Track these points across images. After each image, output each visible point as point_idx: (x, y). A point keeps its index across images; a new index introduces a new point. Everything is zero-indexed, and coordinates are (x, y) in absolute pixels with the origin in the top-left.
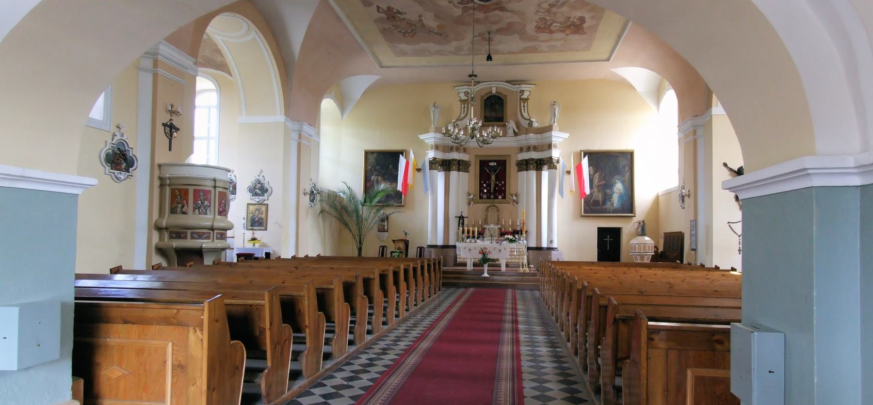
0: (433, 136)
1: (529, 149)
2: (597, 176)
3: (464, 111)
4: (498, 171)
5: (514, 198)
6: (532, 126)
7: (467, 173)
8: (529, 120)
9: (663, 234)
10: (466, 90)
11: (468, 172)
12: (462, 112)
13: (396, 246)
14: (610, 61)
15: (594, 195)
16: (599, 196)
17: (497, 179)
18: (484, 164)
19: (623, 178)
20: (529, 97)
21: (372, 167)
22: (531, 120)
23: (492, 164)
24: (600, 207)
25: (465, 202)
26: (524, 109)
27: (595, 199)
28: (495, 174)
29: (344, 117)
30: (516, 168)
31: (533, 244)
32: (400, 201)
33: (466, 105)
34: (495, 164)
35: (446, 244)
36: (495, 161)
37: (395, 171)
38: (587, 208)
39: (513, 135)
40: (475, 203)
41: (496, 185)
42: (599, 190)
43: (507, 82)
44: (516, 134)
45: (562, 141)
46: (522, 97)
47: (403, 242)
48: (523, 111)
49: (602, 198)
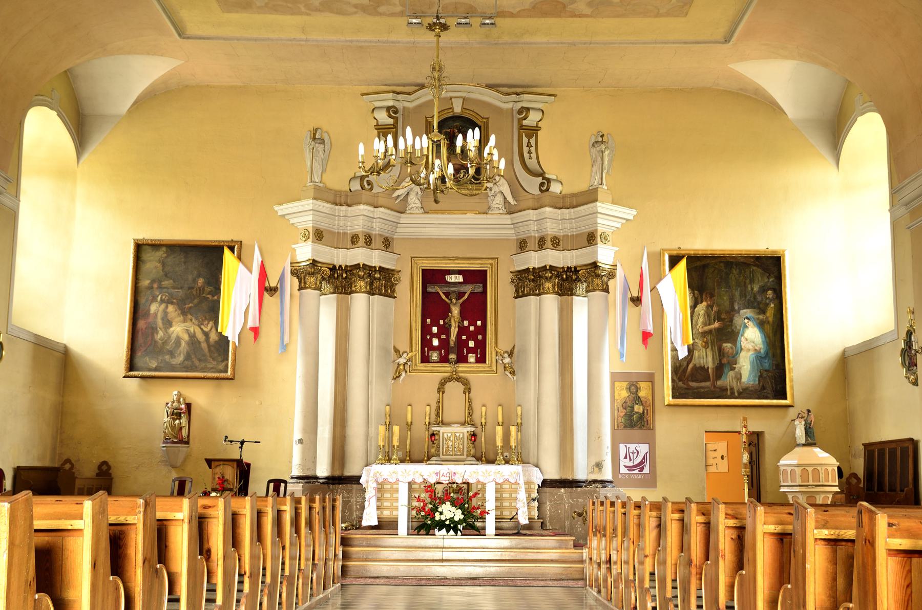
0: (311, 207)
1: (541, 244)
2: (701, 308)
4: (466, 296)
5: (507, 360)
6: (547, 190)
8: (542, 174)
9: (862, 447)
10: (390, 103)
13: (214, 474)
14: (731, 43)
15: (696, 354)
16: (706, 358)
17: (463, 315)
18: (432, 277)
19: (761, 317)
20: (540, 124)
21: (153, 281)
22: (547, 176)
23: (452, 278)
24: (708, 384)
26: (530, 152)
27: (698, 366)
28: (461, 301)
29: (86, 157)
30: (511, 290)
31: (553, 475)
32: (221, 367)
34: (460, 279)
35: (337, 473)
36: (460, 272)
37: (209, 293)
38: (680, 384)
41: (462, 330)
42: (706, 343)
43: (490, 86)
45: (619, 225)
46: (525, 122)
47: (235, 464)
48: (526, 155)
49: (714, 363)
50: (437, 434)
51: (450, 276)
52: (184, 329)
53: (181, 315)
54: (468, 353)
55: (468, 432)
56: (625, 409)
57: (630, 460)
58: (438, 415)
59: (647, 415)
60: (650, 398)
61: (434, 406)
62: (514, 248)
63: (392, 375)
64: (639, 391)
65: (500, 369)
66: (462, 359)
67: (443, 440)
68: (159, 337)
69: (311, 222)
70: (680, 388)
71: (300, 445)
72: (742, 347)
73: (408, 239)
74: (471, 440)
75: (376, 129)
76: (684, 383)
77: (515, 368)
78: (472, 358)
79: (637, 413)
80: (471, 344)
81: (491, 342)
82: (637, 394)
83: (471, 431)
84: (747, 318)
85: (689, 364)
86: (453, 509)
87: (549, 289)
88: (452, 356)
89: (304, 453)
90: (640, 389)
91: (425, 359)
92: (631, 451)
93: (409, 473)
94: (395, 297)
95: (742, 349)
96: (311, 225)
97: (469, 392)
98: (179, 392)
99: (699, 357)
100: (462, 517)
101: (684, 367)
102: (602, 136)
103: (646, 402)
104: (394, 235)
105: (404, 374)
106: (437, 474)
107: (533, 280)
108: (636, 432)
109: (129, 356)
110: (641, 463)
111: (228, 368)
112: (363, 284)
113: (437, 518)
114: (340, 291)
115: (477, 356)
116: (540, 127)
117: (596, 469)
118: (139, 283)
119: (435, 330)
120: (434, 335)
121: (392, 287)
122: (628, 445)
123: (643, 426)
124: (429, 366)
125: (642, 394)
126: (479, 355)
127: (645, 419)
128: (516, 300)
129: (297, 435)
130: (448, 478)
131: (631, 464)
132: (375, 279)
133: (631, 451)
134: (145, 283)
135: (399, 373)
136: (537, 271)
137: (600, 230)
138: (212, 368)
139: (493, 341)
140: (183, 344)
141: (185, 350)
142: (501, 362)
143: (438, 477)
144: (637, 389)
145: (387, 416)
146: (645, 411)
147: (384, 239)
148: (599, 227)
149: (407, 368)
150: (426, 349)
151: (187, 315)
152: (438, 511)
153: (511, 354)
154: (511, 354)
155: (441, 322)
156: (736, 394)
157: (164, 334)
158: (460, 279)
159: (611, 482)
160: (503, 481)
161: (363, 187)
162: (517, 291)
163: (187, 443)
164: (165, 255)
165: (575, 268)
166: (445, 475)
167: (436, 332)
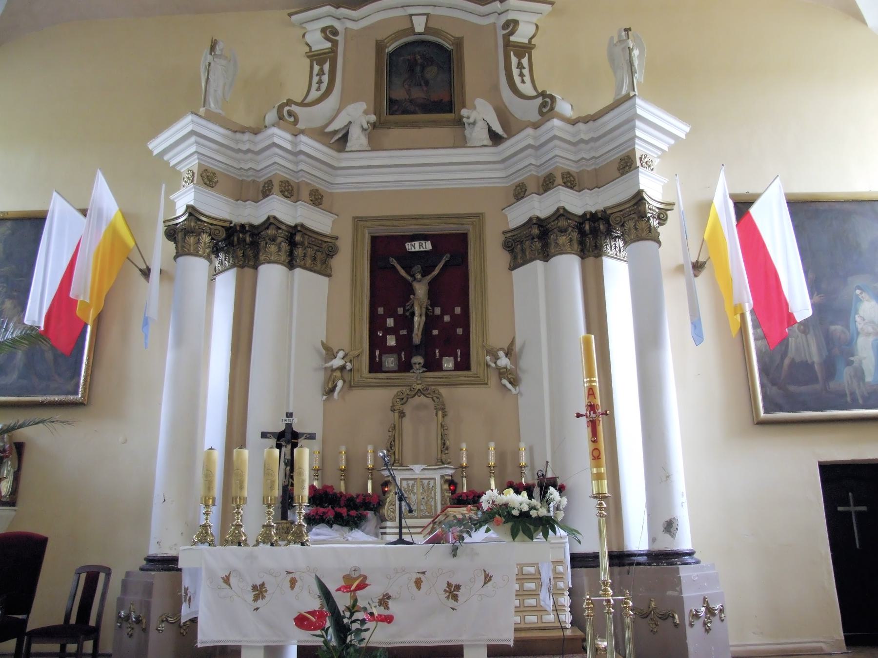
1: (547, 184)
3: (320, 82)
5: (504, 361)
7: (326, 279)
10: (328, 22)
11: (326, 272)
12: (315, 86)
20: (533, 41)
23: (415, 247)
24: (818, 387)
25: (318, 379)
26: (521, 75)
27: (798, 360)
28: (429, 278)
30: (505, 258)
32: (70, 387)
33: (326, 67)
39: (487, 141)
40: (350, 386)
41: (431, 321)
44: (495, 138)
46: (512, 38)
48: (517, 79)
51: (413, 243)
54: (441, 356)
69: (196, 156)
72: (859, 330)
75: (308, 57)
84: (859, 288)
88: (418, 360)
95: (858, 334)
96: (197, 161)
97: (444, 415)
102: (627, 30)
111: (78, 387)
116: (535, 45)
119: (390, 322)
120: (388, 331)
137: (640, 149)
148: (638, 144)
150: (377, 353)
156: (861, 401)
158: (428, 246)
161: (281, 118)
162: (514, 258)
165: (604, 211)
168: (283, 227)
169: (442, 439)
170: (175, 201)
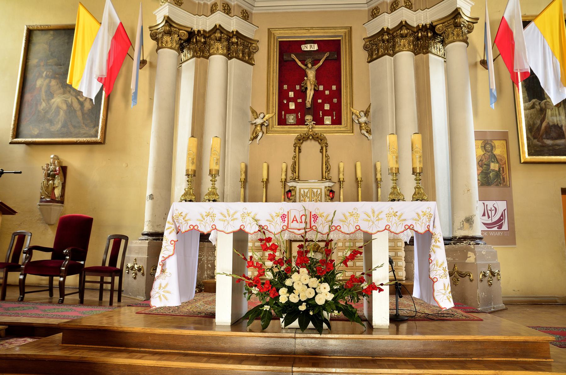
4: (321, 63)
5: (363, 119)
23: (307, 48)
27: (551, 124)
28: (316, 67)
30: (365, 55)
32: (93, 132)
34: (315, 47)
38: (535, 141)
41: (317, 95)
50: (293, 190)
51: (306, 45)
52: (63, 100)
53: (62, 88)
54: (323, 116)
55: (326, 187)
56: (481, 166)
57: (489, 217)
58: (294, 171)
59: (503, 172)
60: (506, 156)
61: (290, 162)
62: (366, 17)
63: (250, 136)
64: (494, 149)
65: (356, 127)
66: (319, 121)
67: (300, 195)
68: (42, 107)
70: (536, 145)
71: (150, 201)
73: (266, 13)
74: (329, 196)
76: (538, 141)
77: (371, 126)
78: (328, 120)
79: (493, 170)
80: (327, 107)
81: (347, 103)
82: (492, 152)
83: (329, 187)
85: (543, 122)
86: (314, 282)
87: (404, 46)
88: (309, 118)
89: (154, 209)
90: (495, 147)
91: (282, 122)
92: (489, 208)
93: (235, 217)
94: (253, 65)
98: (55, 156)
99: (552, 115)
100: (330, 297)
101: (537, 125)
103: (501, 160)
104: (253, 10)
105: (260, 134)
106: (283, 217)
107: (388, 40)
108: (493, 190)
109: (16, 125)
110: (500, 220)
111: (98, 133)
112: (219, 45)
113: (283, 299)
114: (198, 55)
115: (332, 118)
117: (466, 225)
118: (28, 62)
119: (291, 94)
120: (290, 100)
121: (250, 54)
122: (486, 203)
123: (500, 183)
124: (286, 128)
125: (497, 152)
126: (334, 117)
127: (501, 177)
128: (370, 64)
129: (149, 191)
130: (303, 225)
131: (490, 222)
132: (233, 43)
133: (489, 208)
134: (33, 61)
135: (256, 133)
136: (391, 33)
138: (84, 134)
139: (349, 102)
140: (62, 113)
141: (63, 118)
142: (357, 122)
143: (286, 223)
144: (493, 147)
145: (242, 172)
146: (501, 169)
147: (243, 10)
149: (264, 128)
150: (283, 113)
151: (66, 88)
152: (285, 286)
153: (367, 113)
154: (367, 113)
155: (298, 87)
157: (47, 105)
158: (315, 47)
159: (480, 239)
160: (403, 229)
162: (371, 55)
163: (62, 202)
164: (52, 37)
165: (431, 25)
166: (299, 220)
167: (293, 96)
168: (225, 32)
169: (326, 165)
170: (156, 15)
